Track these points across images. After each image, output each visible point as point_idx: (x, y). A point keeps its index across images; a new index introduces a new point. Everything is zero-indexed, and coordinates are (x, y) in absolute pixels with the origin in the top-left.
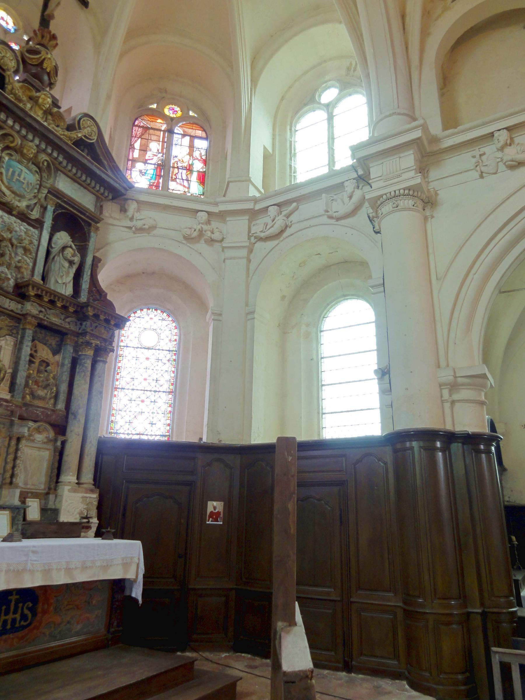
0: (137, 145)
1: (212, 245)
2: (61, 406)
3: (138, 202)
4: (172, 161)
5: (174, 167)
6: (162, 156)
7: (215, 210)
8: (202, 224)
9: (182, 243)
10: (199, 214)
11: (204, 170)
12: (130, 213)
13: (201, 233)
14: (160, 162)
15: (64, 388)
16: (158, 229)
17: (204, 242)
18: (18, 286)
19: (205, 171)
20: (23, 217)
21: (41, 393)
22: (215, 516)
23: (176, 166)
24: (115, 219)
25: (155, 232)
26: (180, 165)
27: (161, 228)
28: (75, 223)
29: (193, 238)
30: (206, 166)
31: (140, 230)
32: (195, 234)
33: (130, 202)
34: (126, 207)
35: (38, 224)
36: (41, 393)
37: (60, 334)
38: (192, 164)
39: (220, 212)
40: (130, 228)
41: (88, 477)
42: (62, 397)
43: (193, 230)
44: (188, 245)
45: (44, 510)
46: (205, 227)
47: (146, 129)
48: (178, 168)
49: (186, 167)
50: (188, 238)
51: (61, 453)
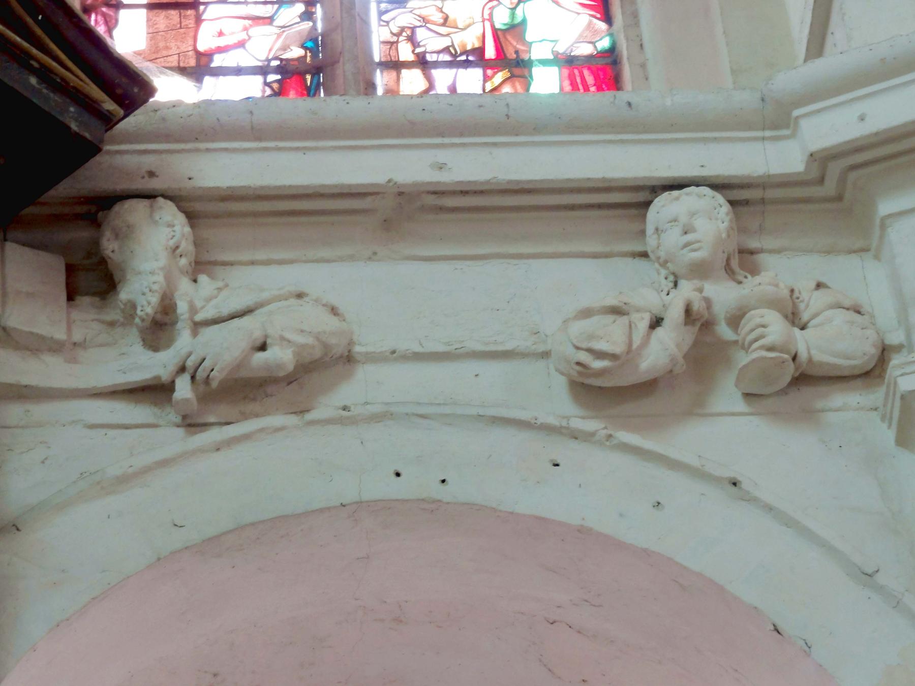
1: (809, 416)
3: (196, 207)
4: (378, 35)
5: (395, 65)
6: (308, 15)
7: (784, 158)
8: (700, 270)
9: (575, 435)
10: (664, 207)
11: (604, 44)
12: (142, 286)
13: (707, 344)
14: (296, 52)
16: (364, 373)
17: (741, 406)
19: (612, 52)
23: (405, 53)
24: (36, 345)
25: (357, 390)
26: (432, 43)
27: (395, 356)
29: (647, 387)
30: (607, 18)
31: (242, 391)
32: (662, 349)
33: (133, 212)
34: (109, 246)
38: (516, 29)
39: (822, 160)
40: (156, 391)
43: (643, 324)
44: (624, 436)
46: (723, 294)
48: (422, 63)
49: (480, 51)
50: (609, 392)
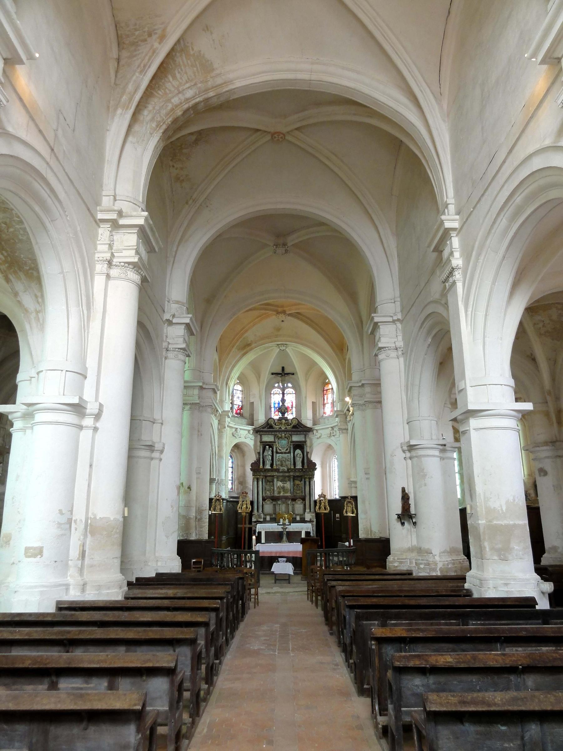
0: (325, 398)
2: (303, 494)
15: (303, 490)
18: (288, 469)
20: (285, 453)
21: (298, 492)
22: (338, 518)
28: (300, 446)
35: (290, 452)
36: (298, 492)
37: (301, 477)
41: (312, 510)
42: (303, 492)
45: (301, 518)
47: (327, 390)
51: (305, 505)
